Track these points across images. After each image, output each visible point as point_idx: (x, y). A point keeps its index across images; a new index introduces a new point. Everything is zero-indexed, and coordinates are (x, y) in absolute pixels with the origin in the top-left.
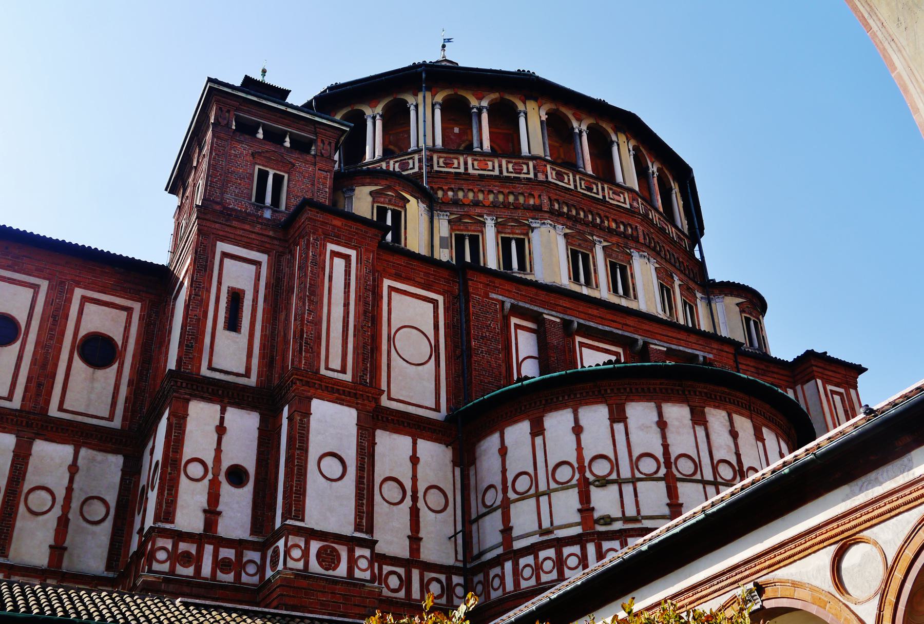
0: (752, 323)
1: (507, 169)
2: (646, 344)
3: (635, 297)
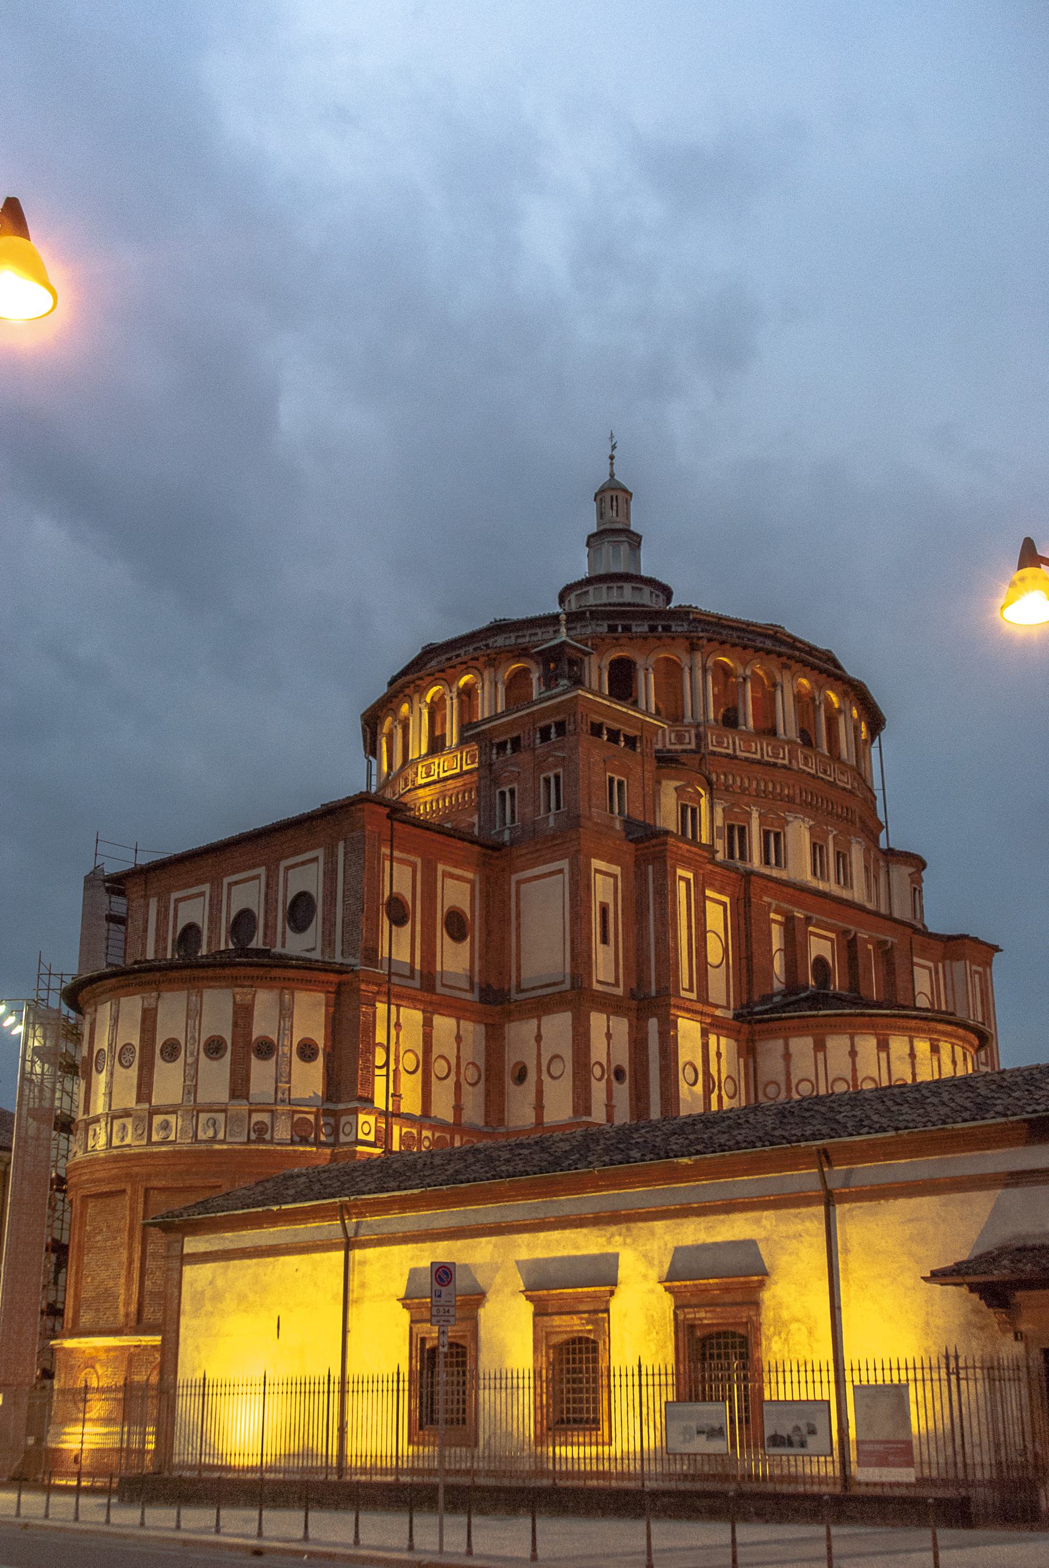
0: (917, 892)
1: (767, 752)
2: (855, 935)
3: (852, 888)
